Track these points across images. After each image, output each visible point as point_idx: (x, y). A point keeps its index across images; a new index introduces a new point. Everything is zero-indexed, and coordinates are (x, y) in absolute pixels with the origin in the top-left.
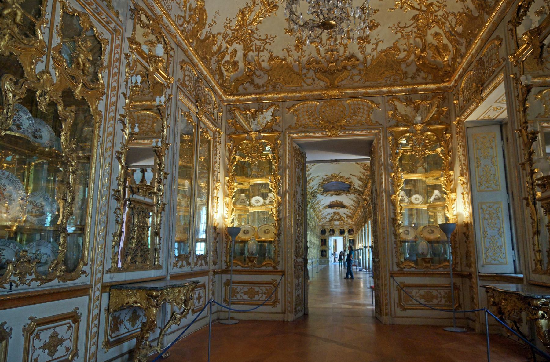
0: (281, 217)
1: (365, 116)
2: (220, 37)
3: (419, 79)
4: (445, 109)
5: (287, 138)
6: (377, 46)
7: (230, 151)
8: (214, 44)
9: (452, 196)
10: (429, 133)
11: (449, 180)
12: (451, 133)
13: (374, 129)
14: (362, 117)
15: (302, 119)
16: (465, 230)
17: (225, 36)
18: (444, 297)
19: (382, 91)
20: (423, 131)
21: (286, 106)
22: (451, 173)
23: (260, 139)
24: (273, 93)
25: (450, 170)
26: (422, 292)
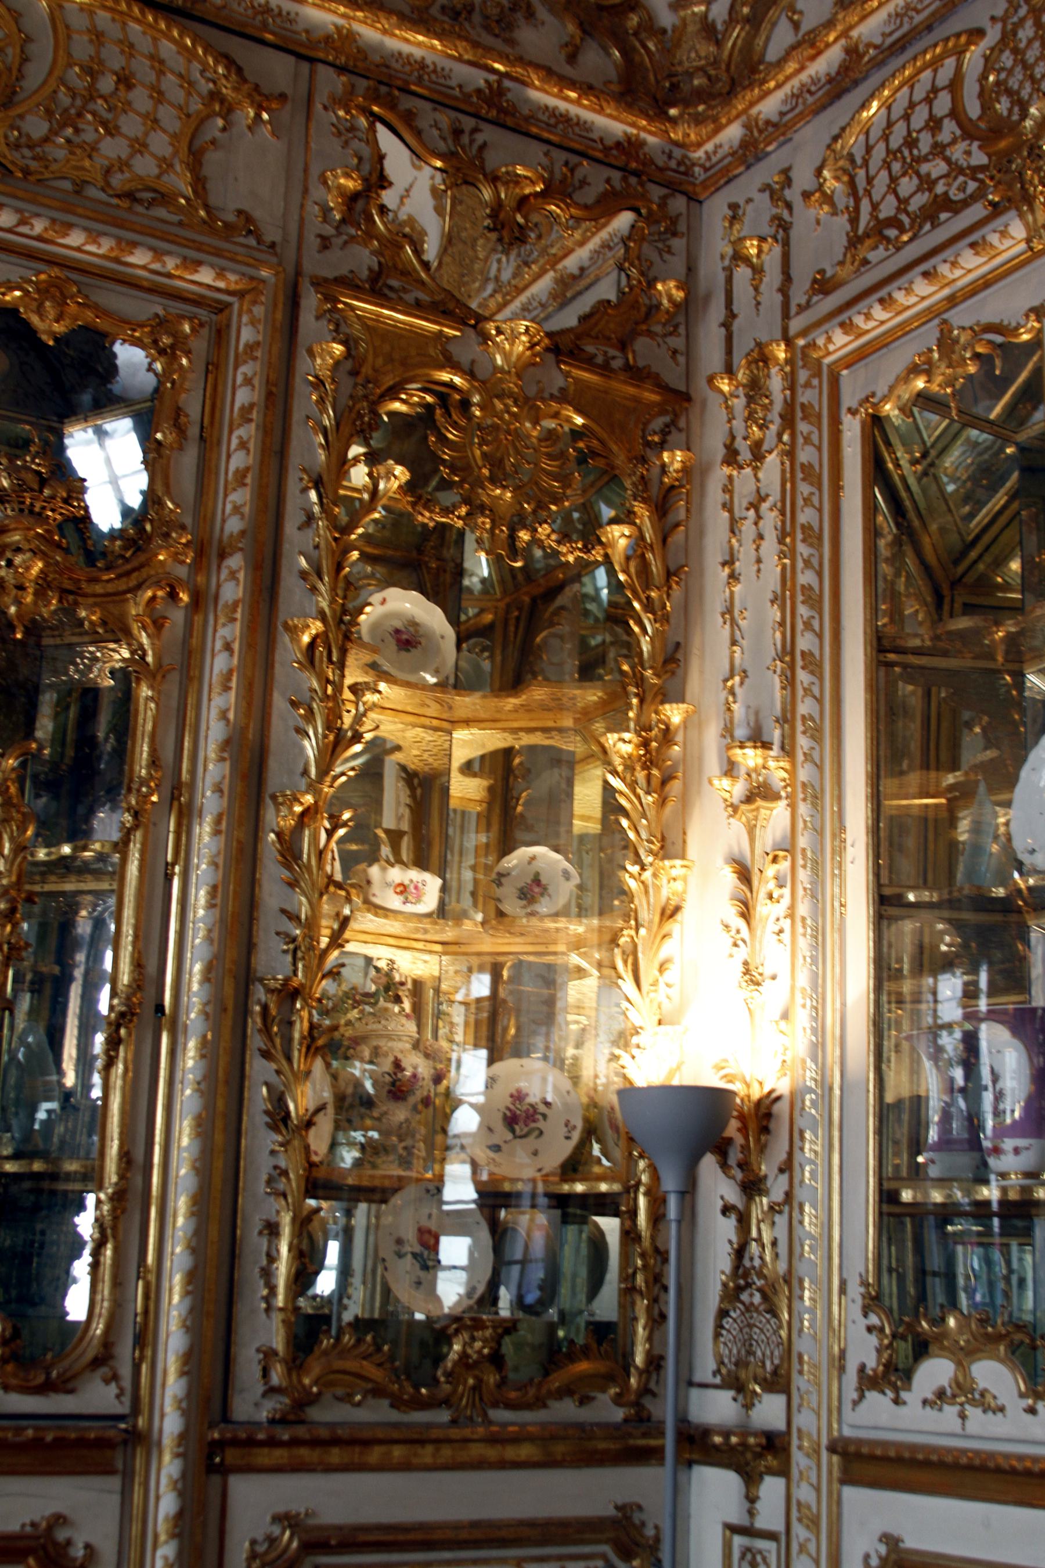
1: (160, 144)
14: (139, 146)
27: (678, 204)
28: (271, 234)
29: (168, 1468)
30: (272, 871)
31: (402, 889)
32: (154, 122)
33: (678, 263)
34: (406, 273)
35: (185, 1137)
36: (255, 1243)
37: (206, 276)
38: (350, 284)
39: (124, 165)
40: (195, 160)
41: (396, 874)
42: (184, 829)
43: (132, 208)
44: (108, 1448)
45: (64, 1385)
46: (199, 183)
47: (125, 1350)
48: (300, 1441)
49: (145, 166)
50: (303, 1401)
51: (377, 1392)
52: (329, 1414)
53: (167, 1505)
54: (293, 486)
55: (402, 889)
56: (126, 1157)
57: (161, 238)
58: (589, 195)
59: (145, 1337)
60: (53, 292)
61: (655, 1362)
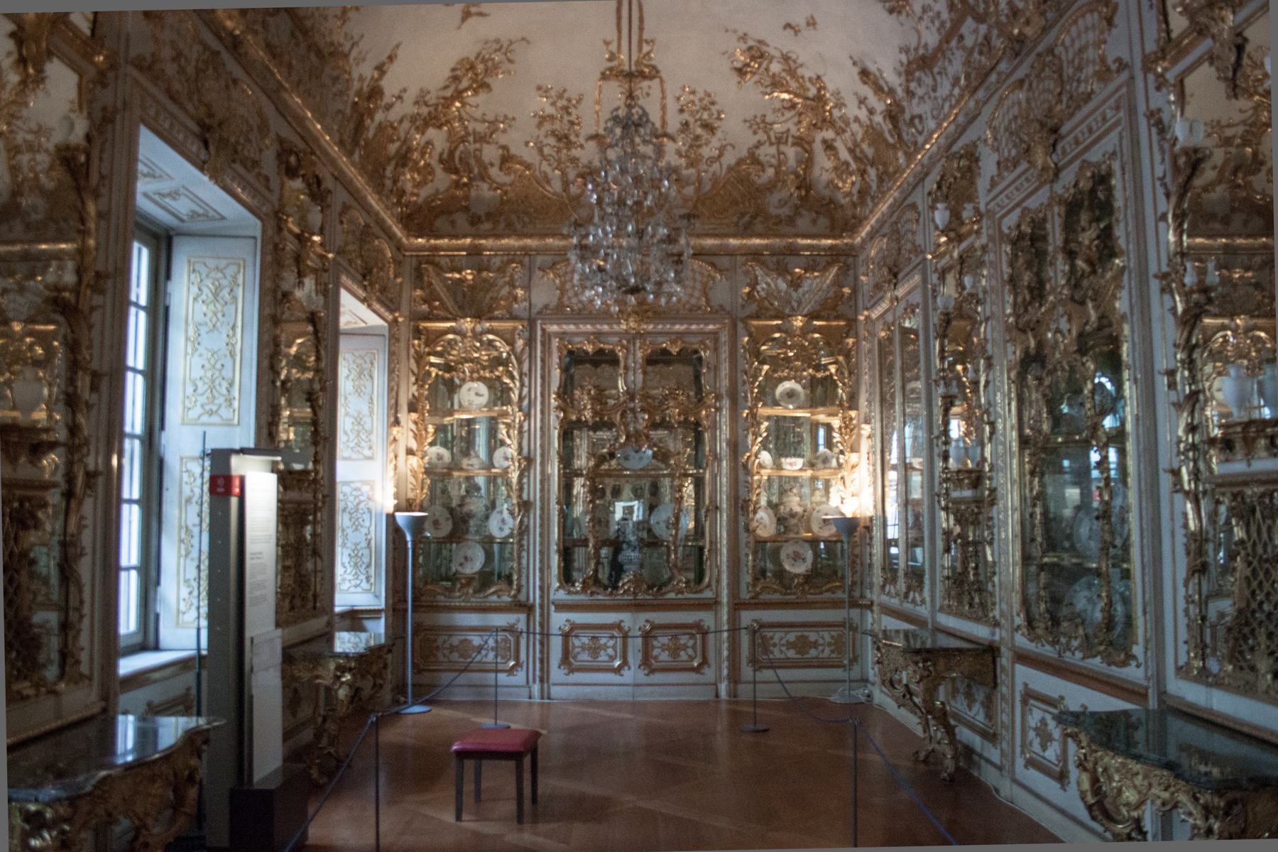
0: (525, 497)
1: (697, 294)
2: (406, 124)
3: (803, 223)
4: (847, 290)
5: (539, 333)
6: (720, 156)
7: (419, 358)
8: (392, 141)
9: (853, 458)
10: (817, 335)
11: (848, 426)
12: (856, 336)
13: (714, 322)
15: (571, 293)
16: (868, 524)
17: (413, 119)
18: (830, 644)
19: (727, 246)
20: (805, 331)
21: (538, 264)
22: (853, 414)
23: (482, 333)
24: (508, 236)
25: (850, 408)
26: (792, 637)
27: (851, 260)
28: (728, 308)
29: (725, 610)
30: (741, 472)
31: (791, 464)
32: (694, 288)
33: (851, 279)
34: (767, 309)
35: (725, 535)
36: (743, 558)
37: (711, 327)
38: (751, 317)
39: (688, 302)
40: (705, 294)
41: (789, 460)
42: (719, 465)
43: (691, 313)
44: (712, 605)
45: (701, 591)
46: (708, 301)
47: (714, 584)
48: (756, 604)
49: (693, 301)
50: (758, 594)
51: (775, 591)
52: (765, 597)
53: (725, 617)
54: (739, 375)
55: (791, 464)
56: (711, 542)
57: (698, 320)
58: (821, 267)
59: (718, 581)
60: (673, 342)
61: (854, 583)
